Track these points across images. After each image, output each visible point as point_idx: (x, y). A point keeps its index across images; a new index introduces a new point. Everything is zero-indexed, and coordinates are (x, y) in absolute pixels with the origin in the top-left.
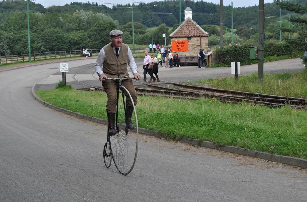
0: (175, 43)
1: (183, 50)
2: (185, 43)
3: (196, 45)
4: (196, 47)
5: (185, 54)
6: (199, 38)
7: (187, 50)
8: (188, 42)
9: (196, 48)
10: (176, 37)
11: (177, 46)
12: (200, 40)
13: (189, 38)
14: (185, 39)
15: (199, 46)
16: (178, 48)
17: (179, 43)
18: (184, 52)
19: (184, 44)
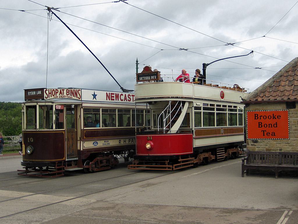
0: (256, 116)
1: (274, 134)
2: (279, 117)
8: (286, 114)
11: (260, 125)
14: (280, 108)
16: (263, 128)
17: (265, 117)
18: (279, 141)
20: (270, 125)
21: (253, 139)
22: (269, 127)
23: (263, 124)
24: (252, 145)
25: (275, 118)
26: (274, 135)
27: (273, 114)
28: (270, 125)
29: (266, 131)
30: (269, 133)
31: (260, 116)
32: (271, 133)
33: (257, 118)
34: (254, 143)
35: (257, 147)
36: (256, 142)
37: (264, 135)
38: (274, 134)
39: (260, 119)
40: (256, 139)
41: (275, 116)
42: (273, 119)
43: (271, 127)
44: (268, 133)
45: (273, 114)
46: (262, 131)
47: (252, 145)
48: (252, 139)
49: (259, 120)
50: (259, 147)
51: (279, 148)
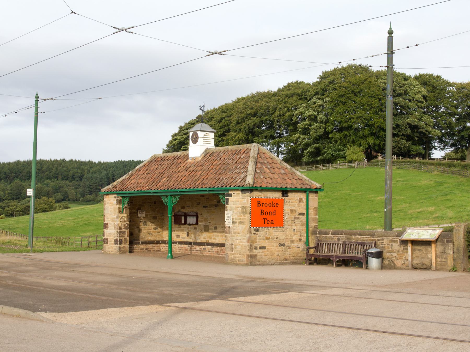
1: (272, 222)
2: (277, 204)
3: (297, 212)
4: (297, 216)
7: (281, 224)
8: (282, 201)
9: (297, 218)
10: (262, 190)
11: (262, 212)
12: (304, 200)
13: (285, 192)
14: (278, 195)
15: (303, 214)
16: (264, 216)
17: (266, 205)
24: (254, 234)
33: (259, 205)
36: (257, 230)
47: (254, 234)
49: (261, 208)
51: (276, 237)
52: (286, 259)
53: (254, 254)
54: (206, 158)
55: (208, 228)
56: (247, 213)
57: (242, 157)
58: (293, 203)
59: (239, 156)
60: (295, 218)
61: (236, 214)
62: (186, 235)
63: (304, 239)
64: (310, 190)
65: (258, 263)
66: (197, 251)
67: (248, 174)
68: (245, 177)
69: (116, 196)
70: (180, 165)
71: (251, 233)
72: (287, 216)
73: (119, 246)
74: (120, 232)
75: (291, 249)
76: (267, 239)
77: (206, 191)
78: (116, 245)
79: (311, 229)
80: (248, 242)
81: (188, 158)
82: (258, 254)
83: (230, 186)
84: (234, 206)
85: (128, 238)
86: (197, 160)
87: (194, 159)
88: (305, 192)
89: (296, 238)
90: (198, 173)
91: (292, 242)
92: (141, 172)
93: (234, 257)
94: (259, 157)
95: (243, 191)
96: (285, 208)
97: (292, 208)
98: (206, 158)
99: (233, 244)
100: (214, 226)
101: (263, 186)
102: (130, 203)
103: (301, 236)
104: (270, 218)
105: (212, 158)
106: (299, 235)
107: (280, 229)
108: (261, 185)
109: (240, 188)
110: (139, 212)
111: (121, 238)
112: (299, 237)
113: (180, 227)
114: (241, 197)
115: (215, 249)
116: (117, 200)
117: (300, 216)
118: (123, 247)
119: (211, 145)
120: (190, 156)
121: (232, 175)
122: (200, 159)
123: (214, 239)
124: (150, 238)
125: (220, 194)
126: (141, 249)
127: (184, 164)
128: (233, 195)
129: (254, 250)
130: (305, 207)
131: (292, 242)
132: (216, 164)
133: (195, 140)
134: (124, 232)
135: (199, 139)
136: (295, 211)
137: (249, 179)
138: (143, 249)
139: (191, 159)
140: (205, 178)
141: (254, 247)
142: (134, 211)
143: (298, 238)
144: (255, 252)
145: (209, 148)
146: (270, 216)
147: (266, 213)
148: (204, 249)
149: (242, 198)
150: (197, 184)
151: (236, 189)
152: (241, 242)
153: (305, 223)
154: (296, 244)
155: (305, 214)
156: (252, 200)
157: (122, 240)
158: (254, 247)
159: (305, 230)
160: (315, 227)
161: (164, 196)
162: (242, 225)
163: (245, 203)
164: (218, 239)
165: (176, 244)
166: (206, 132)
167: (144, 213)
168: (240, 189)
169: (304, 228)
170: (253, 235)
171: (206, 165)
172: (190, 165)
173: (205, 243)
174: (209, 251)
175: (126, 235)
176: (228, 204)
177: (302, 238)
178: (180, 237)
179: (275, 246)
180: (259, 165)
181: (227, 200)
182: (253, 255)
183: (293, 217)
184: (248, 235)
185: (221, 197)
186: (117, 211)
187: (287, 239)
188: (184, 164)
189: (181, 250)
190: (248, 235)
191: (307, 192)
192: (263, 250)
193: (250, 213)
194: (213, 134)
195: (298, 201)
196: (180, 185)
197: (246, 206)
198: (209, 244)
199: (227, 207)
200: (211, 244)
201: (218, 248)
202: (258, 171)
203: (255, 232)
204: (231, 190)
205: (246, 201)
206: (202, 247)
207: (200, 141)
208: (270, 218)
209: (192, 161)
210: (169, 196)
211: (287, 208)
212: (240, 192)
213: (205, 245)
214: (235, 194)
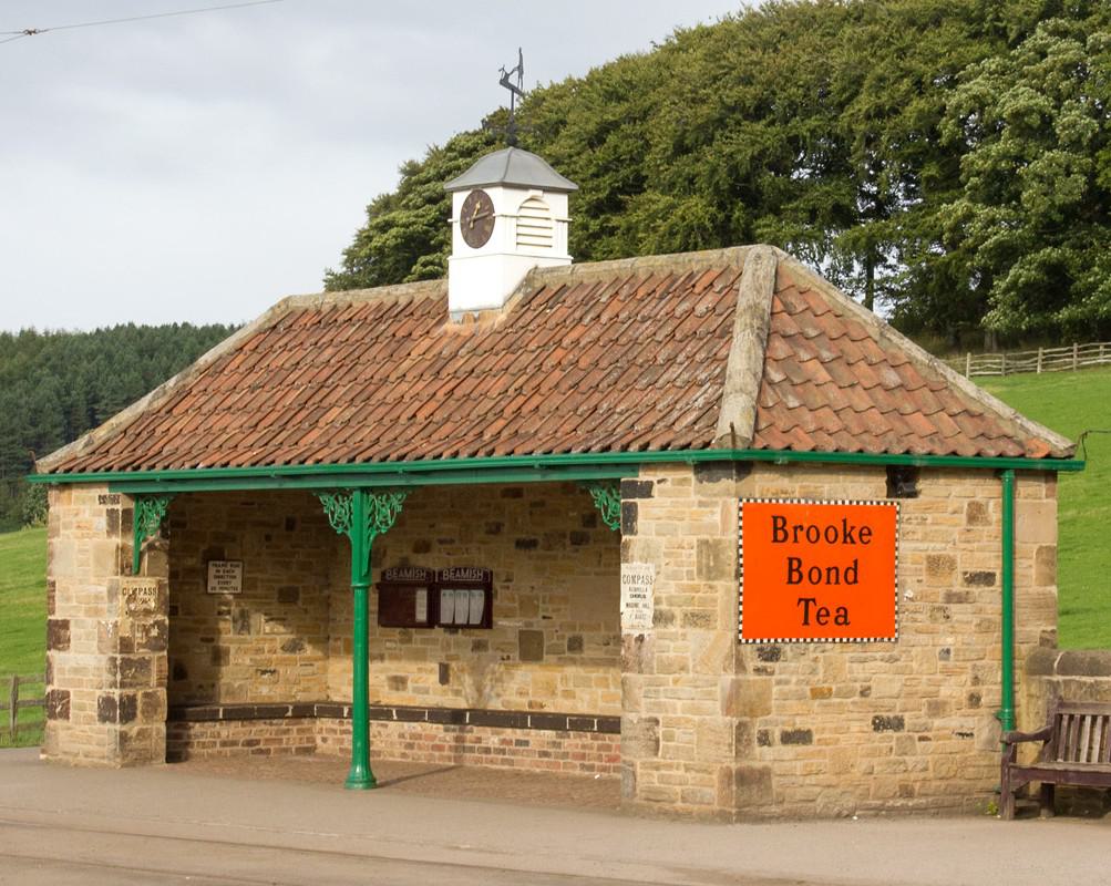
1: (843, 618)
2: (865, 533)
3: (960, 568)
4: (958, 586)
5: (860, 671)
6: (987, 492)
7: (882, 625)
8: (891, 515)
9: (961, 599)
10: (795, 464)
11: (794, 568)
12: (994, 512)
13: (902, 476)
14: (870, 489)
15: (988, 578)
17: (814, 534)
19: (855, 551)
20: (833, 572)
21: (762, 641)
22: (828, 582)
23: (805, 570)
24: (758, 670)
25: (853, 542)
26: (846, 623)
27: (845, 521)
28: (833, 572)
29: (814, 600)
30: (828, 615)
31: (795, 528)
32: (835, 611)
34: (766, 660)
35: (779, 682)
36: (772, 655)
37: (806, 623)
38: (845, 617)
39: (796, 541)
40: (776, 640)
41: (853, 528)
42: (845, 542)
43: (837, 582)
44: (823, 612)
45: (845, 521)
46: (800, 600)
47: (758, 670)
48: (758, 641)
49: (789, 550)
50: (787, 682)
51: (858, 686)
52: (907, 792)
53: (757, 765)
54: (530, 315)
55: (540, 644)
56: (721, 574)
57: (701, 308)
58: (941, 526)
59: (686, 306)
60: (951, 598)
61: (675, 576)
62: (436, 677)
63: (992, 694)
64: (1022, 464)
65: (775, 809)
66: (487, 750)
67: (728, 387)
68: (715, 404)
69: (105, 491)
70: (409, 345)
71: (740, 666)
72: (912, 586)
73: (118, 727)
74: (127, 664)
75: (933, 744)
76: (818, 694)
77: (529, 468)
78: (108, 726)
79: (1023, 650)
80: (728, 711)
81: (443, 316)
82: (776, 768)
83: (644, 448)
84: (663, 541)
85: (162, 693)
86: (486, 325)
87: (475, 316)
88: (997, 473)
89: (954, 690)
90: (495, 386)
91: (937, 708)
92: (224, 382)
93: (662, 779)
94: (779, 307)
95: (707, 467)
96: (905, 548)
97: (936, 548)
98: (530, 315)
99: (657, 722)
100: (569, 634)
101: (798, 447)
102: (171, 526)
103: (976, 680)
104: (829, 596)
105: (559, 313)
106: (967, 677)
107: (878, 650)
108: (787, 439)
109: (691, 456)
110: (212, 571)
111: (130, 692)
112: (969, 688)
113: (409, 641)
114: (695, 498)
115: (573, 741)
116: (111, 513)
117: (975, 590)
118: (141, 733)
119: (557, 252)
120: (452, 306)
121: (652, 396)
122: (502, 317)
123: (568, 694)
124: (265, 691)
125: (596, 482)
126: (224, 744)
127: (427, 343)
128: (656, 487)
129: (758, 749)
130: (997, 544)
131: (937, 708)
132: (577, 341)
133: (479, 231)
134: (143, 664)
135: (498, 221)
136: (952, 563)
137: (735, 415)
138: (234, 743)
139: (458, 317)
140: (525, 410)
141: (755, 732)
142: (191, 562)
143: (962, 694)
144: (762, 757)
145: (543, 264)
146: (833, 586)
147: (815, 576)
148: (519, 743)
149: (701, 504)
150: (487, 437)
151: (669, 461)
152: (697, 711)
153: (998, 619)
154: (955, 722)
155: (998, 578)
156: (749, 512)
157: (132, 700)
158: (755, 732)
159: (998, 655)
160: (1044, 641)
161: (330, 491)
162: (698, 631)
163: (713, 526)
164: (587, 697)
165: (389, 716)
166: (532, 193)
167: (238, 572)
168: (690, 460)
169: (993, 643)
170: (752, 677)
171: (532, 346)
172: (455, 345)
173: (524, 715)
174: (545, 754)
175: (154, 679)
176: (632, 531)
177: (983, 689)
178: (410, 684)
179: (855, 726)
180: (781, 348)
181: (630, 513)
182: (752, 771)
183: (942, 591)
184: (730, 677)
185: (600, 497)
186: (111, 564)
187: (910, 695)
188: (427, 343)
189: (410, 746)
190: (730, 677)
191: (1008, 476)
192: (800, 748)
193: (738, 575)
194: (563, 200)
195: (963, 517)
196: (408, 442)
197: (717, 543)
198: (544, 721)
199: (627, 545)
200: (556, 722)
201: (587, 739)
202: (777, 377)
203: (761, 664)
204: (649, 466)
205: (717, 518)
206: (509, 733)
207: (502, 231)
208: (829, 596)
209: (466, 330)
210: (356, 495)
211: (911, 550)
212: (690, 475)
213: (524, 726)
214: (668, 485)
